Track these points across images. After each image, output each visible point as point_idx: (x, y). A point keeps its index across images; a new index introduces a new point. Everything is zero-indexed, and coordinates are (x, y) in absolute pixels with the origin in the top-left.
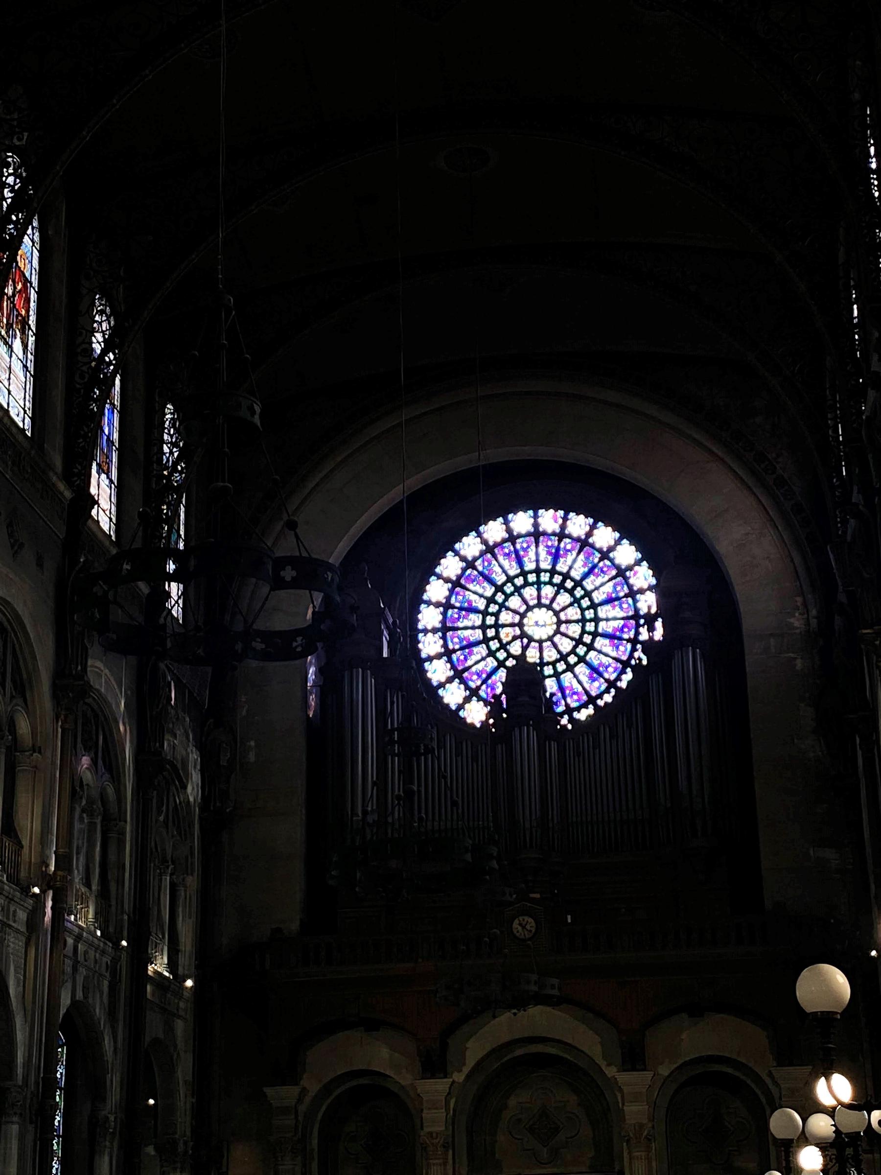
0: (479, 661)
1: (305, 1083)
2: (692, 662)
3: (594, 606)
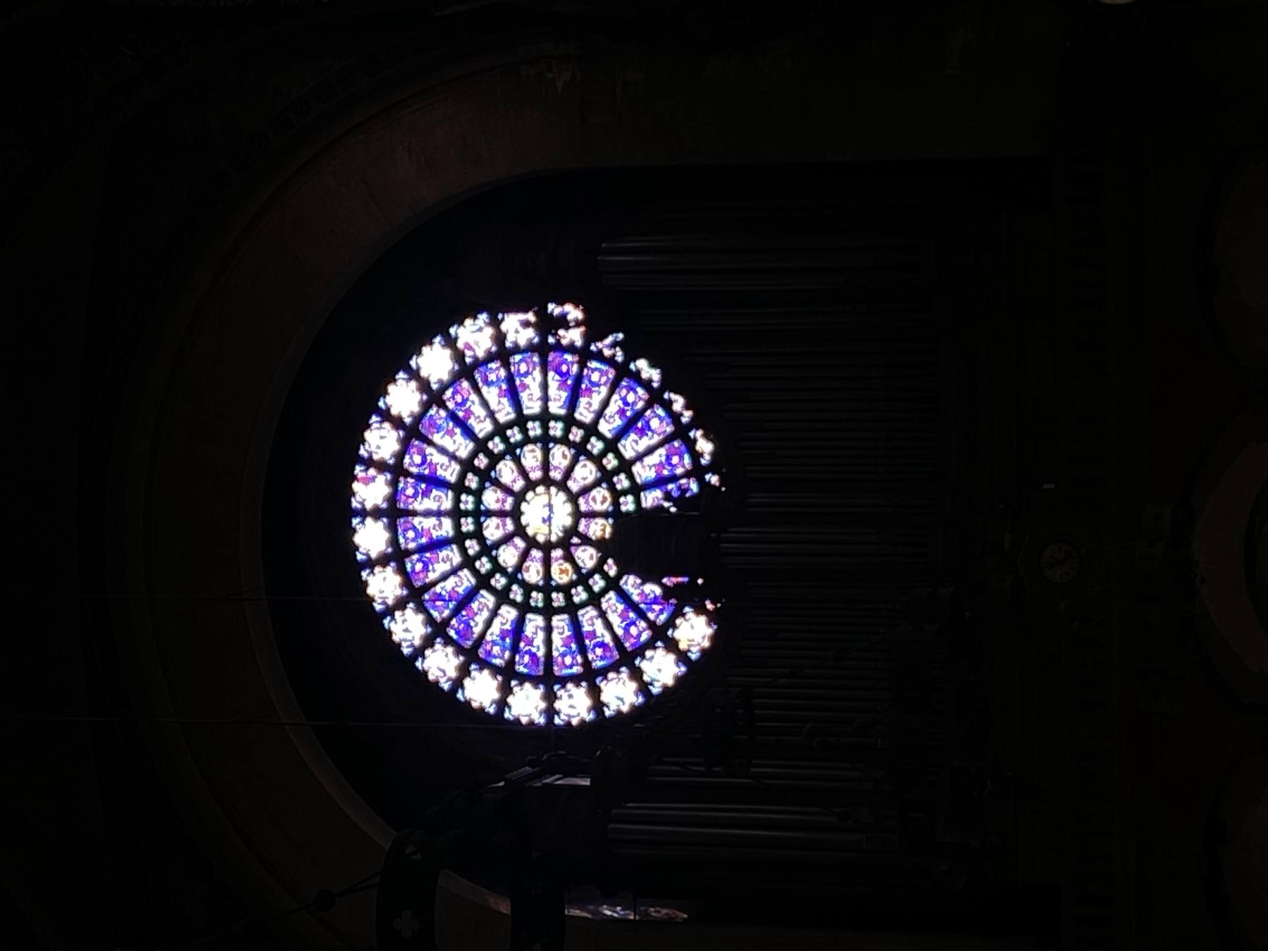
0: (606, 622)
3: (521, 420)
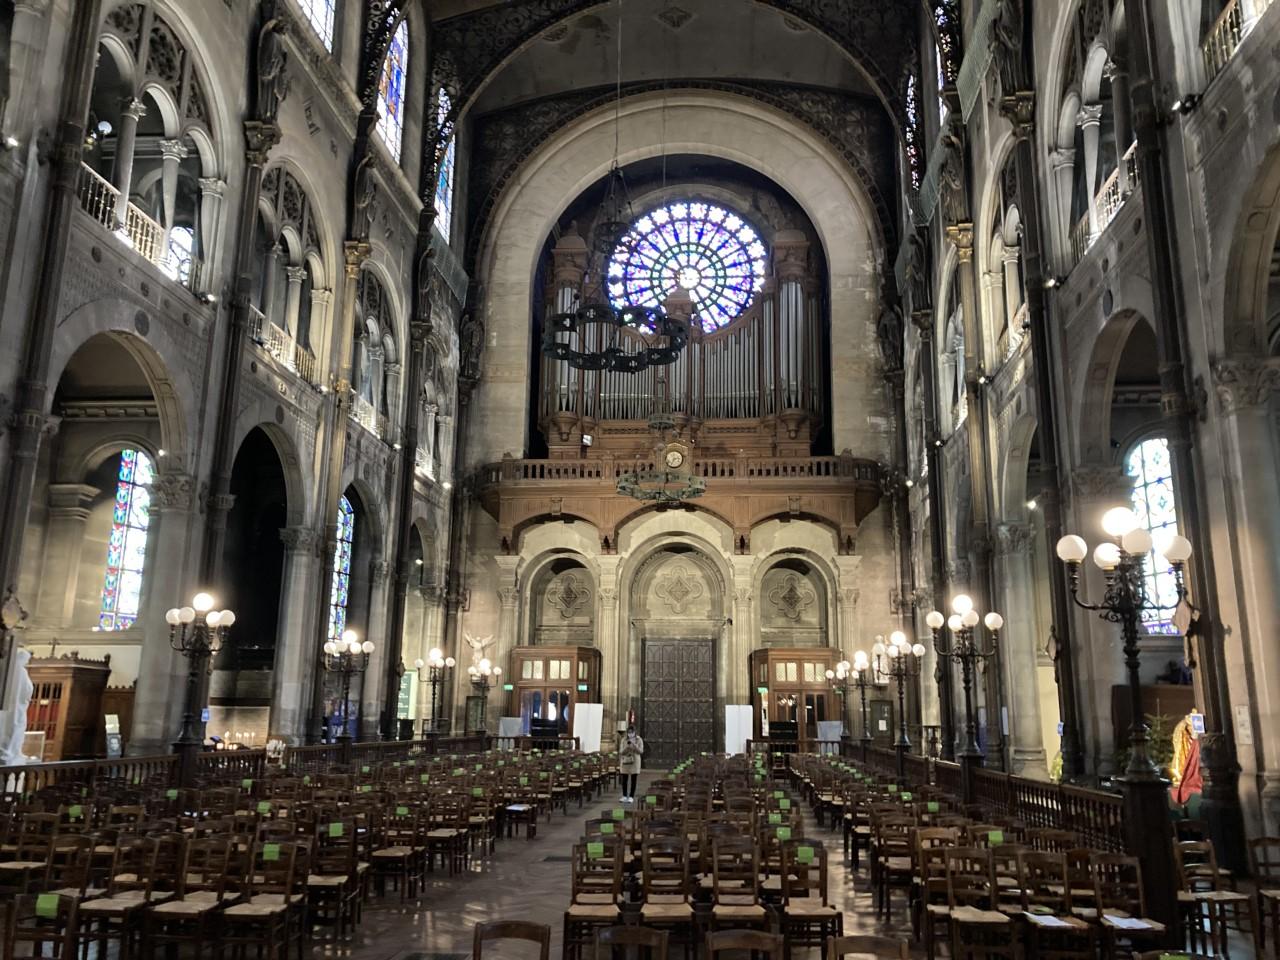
1: (524, 553)
2: (793, 295)
3: (724, 268)
